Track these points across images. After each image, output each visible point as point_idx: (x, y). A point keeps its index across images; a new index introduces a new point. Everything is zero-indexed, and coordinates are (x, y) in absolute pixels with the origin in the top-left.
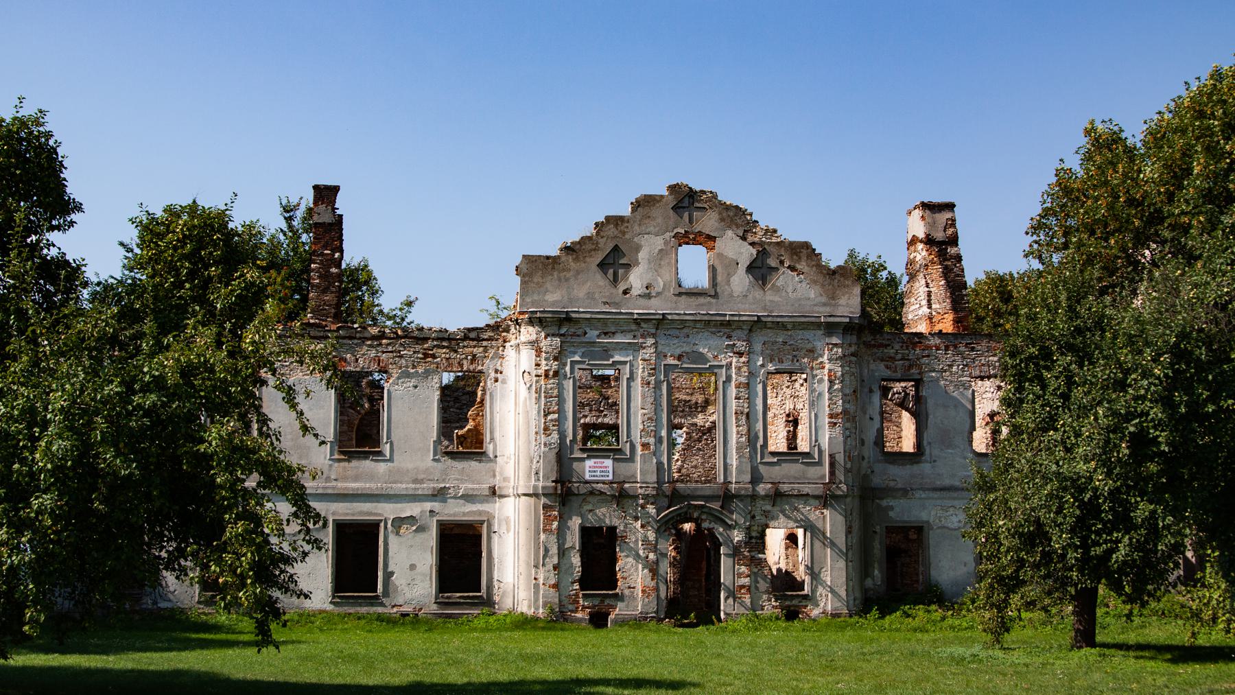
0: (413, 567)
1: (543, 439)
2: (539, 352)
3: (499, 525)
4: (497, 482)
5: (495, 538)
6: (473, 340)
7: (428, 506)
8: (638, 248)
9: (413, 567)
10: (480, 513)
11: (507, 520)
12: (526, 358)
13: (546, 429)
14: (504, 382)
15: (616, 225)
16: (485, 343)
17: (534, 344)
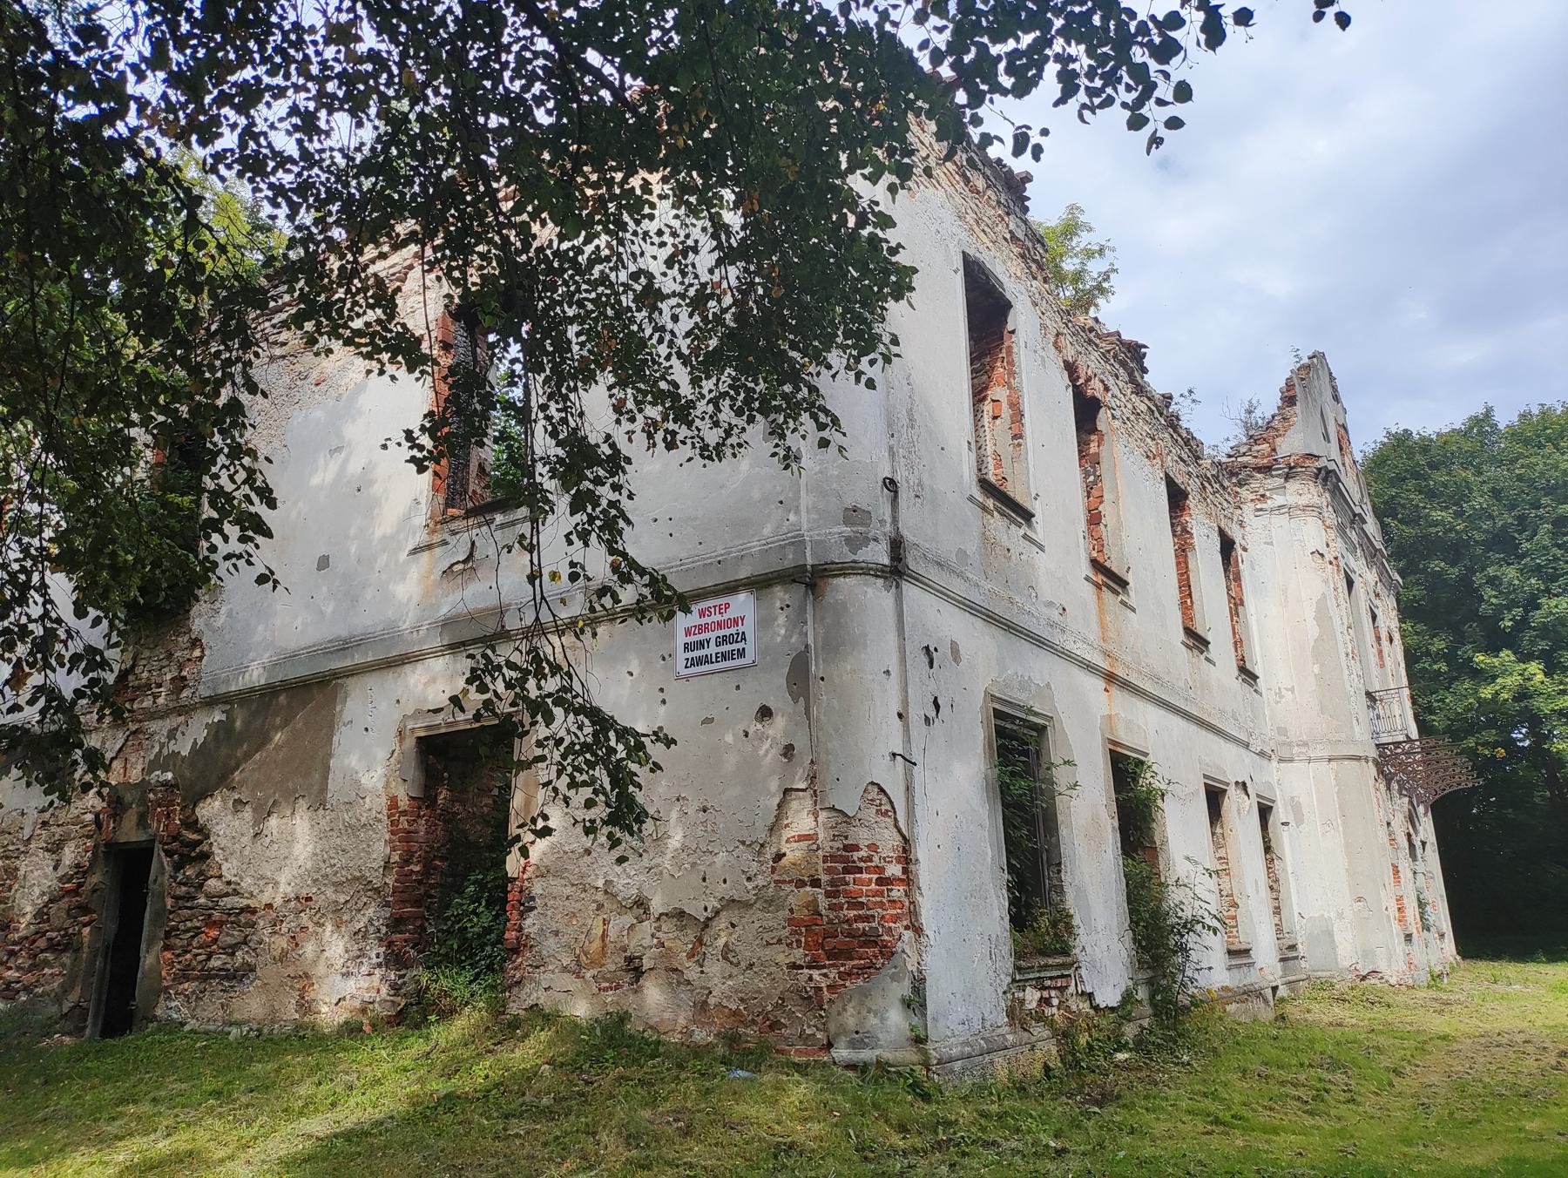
11: (1296, 807)
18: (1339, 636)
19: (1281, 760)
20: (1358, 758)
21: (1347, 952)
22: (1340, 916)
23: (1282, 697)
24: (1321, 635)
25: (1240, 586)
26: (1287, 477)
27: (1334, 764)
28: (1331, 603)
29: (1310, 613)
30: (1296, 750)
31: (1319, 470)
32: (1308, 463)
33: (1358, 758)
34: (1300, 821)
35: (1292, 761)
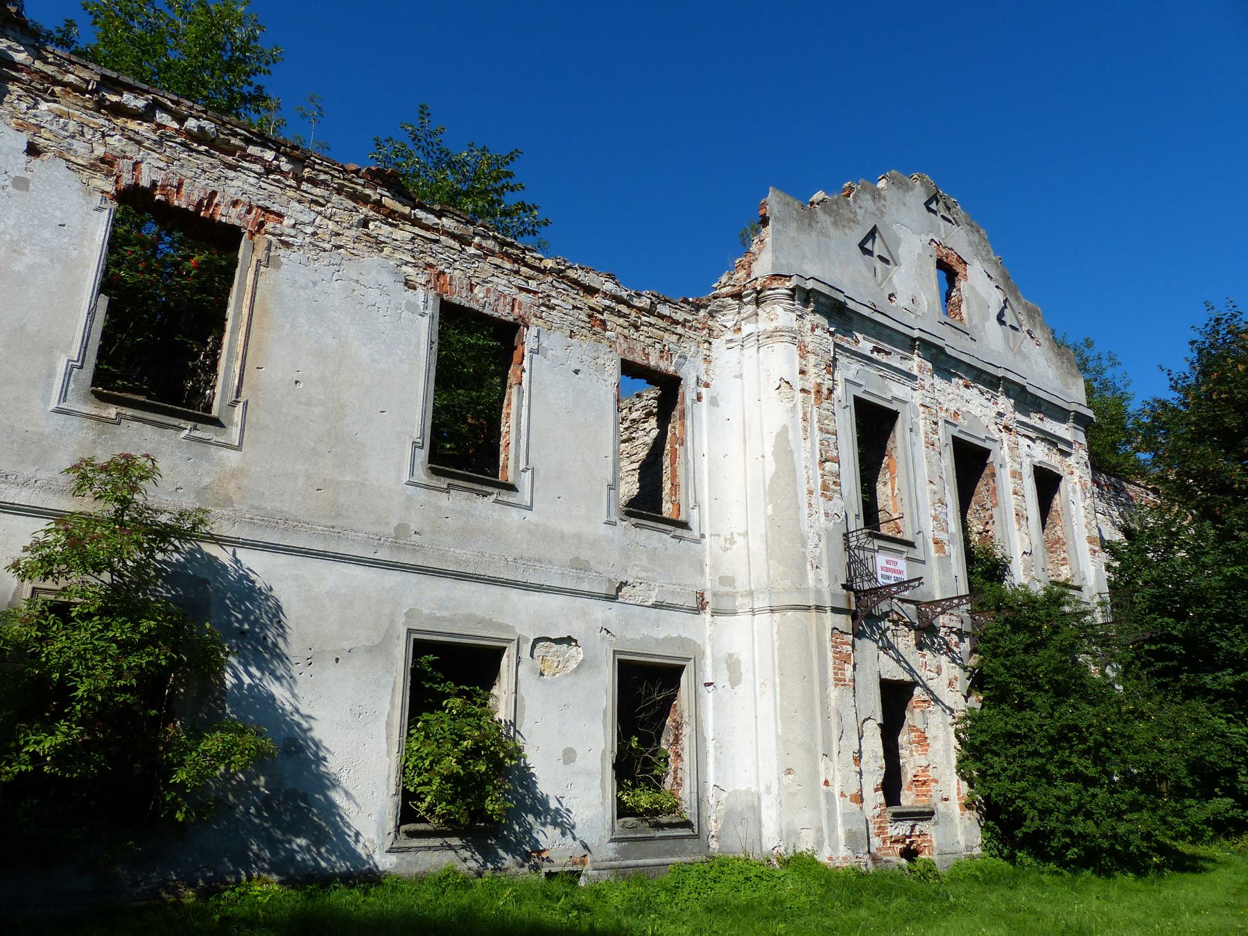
0: (569, 756)
1: (820, 503)
2: (804, 352)
3: (715, 670)
4: (708, 583)
5: (709, 697)
6: (662, 317)
7: (601, 612)
8: (898, 243)
9: (569, 756)
10: (683, 642)
11: (733, 666)
12: (780, 360)
13: (825, 487)
14: (714, 402)
15: (874, 198)
16: (679, 329)
17: (795, 336)
18: (802, 474)
19: (715, 613)
20: (808, 608)
21: (771, 837)
22: (768, 789)
23: (732, 542)
24: (776, 473)
25: (683, 425)
26: (758, 302)
27: (777, 616)
28: (796, 436)
29: (769, 449)
30: (739, 601)
31: (792, 290)
32: (775, 284)
33: (808, 608)
34: (735, 681)
35: (734, 613)
